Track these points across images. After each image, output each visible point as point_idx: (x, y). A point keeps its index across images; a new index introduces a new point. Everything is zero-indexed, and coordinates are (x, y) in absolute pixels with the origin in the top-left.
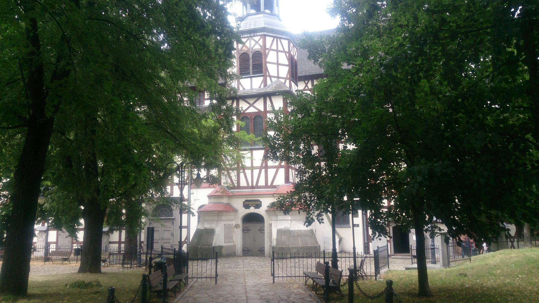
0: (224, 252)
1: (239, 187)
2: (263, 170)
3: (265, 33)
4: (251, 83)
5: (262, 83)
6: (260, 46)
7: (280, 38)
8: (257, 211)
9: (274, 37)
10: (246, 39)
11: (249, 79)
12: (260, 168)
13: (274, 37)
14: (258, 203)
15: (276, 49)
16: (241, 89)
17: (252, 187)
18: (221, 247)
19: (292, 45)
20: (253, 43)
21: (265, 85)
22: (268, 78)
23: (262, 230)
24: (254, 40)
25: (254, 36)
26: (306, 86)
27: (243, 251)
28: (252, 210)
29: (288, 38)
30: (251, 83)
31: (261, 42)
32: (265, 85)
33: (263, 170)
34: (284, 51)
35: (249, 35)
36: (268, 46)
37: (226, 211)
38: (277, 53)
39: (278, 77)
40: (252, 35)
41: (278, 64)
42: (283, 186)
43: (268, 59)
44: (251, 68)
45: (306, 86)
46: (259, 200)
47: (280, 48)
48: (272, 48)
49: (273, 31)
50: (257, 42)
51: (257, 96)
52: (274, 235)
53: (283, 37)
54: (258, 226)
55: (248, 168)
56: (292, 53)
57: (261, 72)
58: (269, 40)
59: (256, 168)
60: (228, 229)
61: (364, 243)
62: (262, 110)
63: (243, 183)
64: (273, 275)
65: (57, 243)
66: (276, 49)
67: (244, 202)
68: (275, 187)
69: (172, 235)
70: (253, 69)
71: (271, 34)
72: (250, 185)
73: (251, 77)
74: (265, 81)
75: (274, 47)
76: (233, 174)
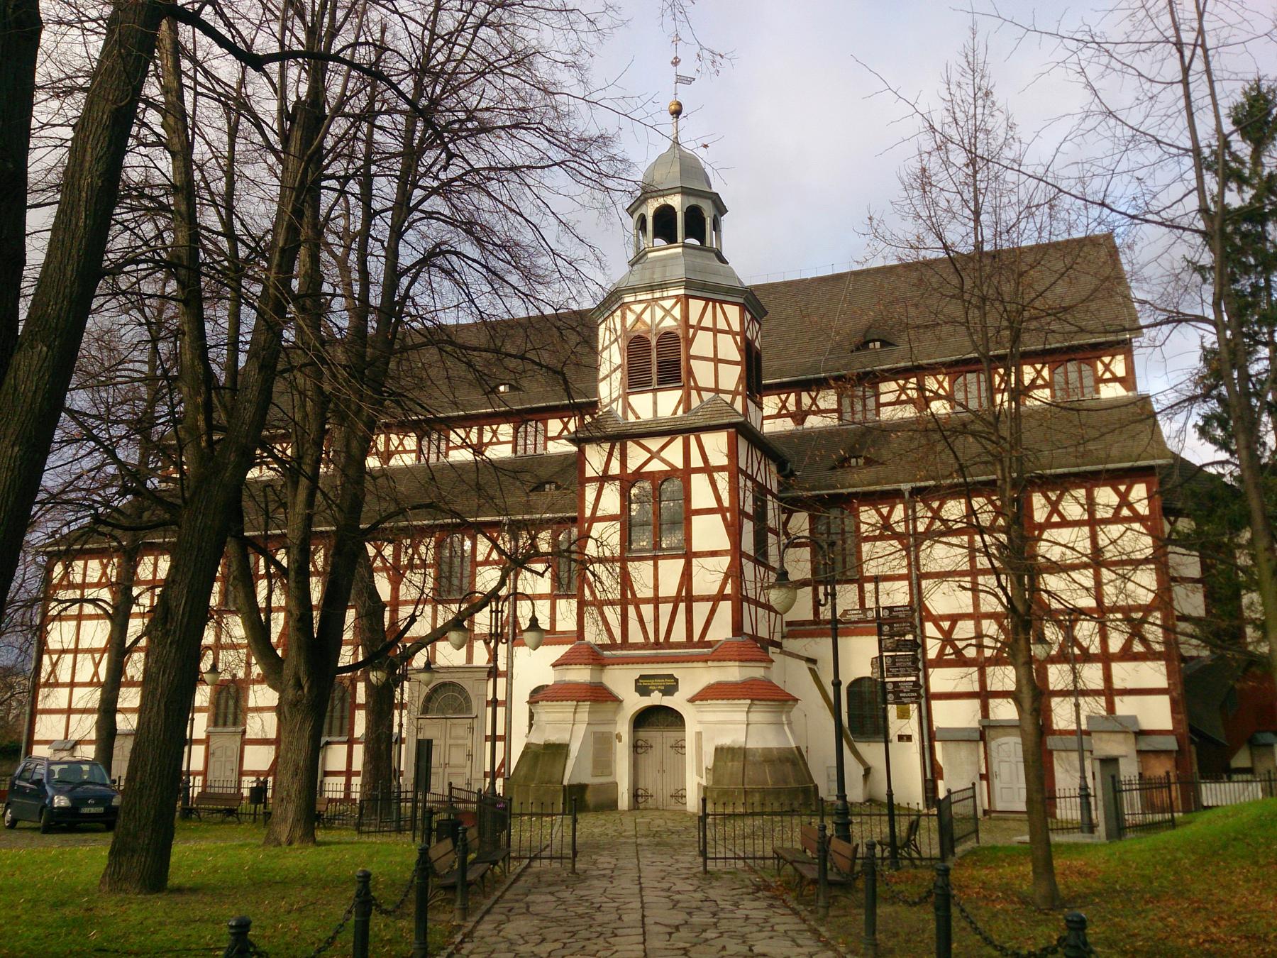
0: (590, 798)
1: (625, 644)
2: (682, 606)
4: (655, 403)
5: (679, 403)
6: (676, 319)
7: (721, 302)
8: (667, 701)
10: (643, 306)
11: (650, 395)
12: (676, 601)
13: (707, 300)
14: (670, 682)
16: (632, 418)
18: (582, 788)
19: (749, 316)
20: (659, 313)
22: (694, 393)
23: (679, 747)
25: (663, 298)
28: (656, 699)
30: (655, 403)
31: (677, 312)
32: (687, 409)
33: (682, 606)
36: (693, 321)
38: (715, 336)
39: (717, 390)
40: (657, 295)
41: (716, 361)
42: (727, 642)
43: (692, 352)
46: (671, 676)
47: (722, 325)
49: (704, 287)
50: (668, 312)
51: (669, 431)
52: (708, 760)
54: (671, 736)
55: (647, 601)
56: (748, 335)
57: (679, 380)
60: (602, 745)
61: (925, 781)
62: (680, 465)
63: (635, 636)
64: (703, 853)
65: (204, 773)
67: (637, 681)
68: (709, 644)
69: (470, 756)
70: (660, 372)
71: (698, 294)
72: (652, 639)
73: (654, 391)
74: (686, 400)
75: (707, 322)
76: (613, 615)
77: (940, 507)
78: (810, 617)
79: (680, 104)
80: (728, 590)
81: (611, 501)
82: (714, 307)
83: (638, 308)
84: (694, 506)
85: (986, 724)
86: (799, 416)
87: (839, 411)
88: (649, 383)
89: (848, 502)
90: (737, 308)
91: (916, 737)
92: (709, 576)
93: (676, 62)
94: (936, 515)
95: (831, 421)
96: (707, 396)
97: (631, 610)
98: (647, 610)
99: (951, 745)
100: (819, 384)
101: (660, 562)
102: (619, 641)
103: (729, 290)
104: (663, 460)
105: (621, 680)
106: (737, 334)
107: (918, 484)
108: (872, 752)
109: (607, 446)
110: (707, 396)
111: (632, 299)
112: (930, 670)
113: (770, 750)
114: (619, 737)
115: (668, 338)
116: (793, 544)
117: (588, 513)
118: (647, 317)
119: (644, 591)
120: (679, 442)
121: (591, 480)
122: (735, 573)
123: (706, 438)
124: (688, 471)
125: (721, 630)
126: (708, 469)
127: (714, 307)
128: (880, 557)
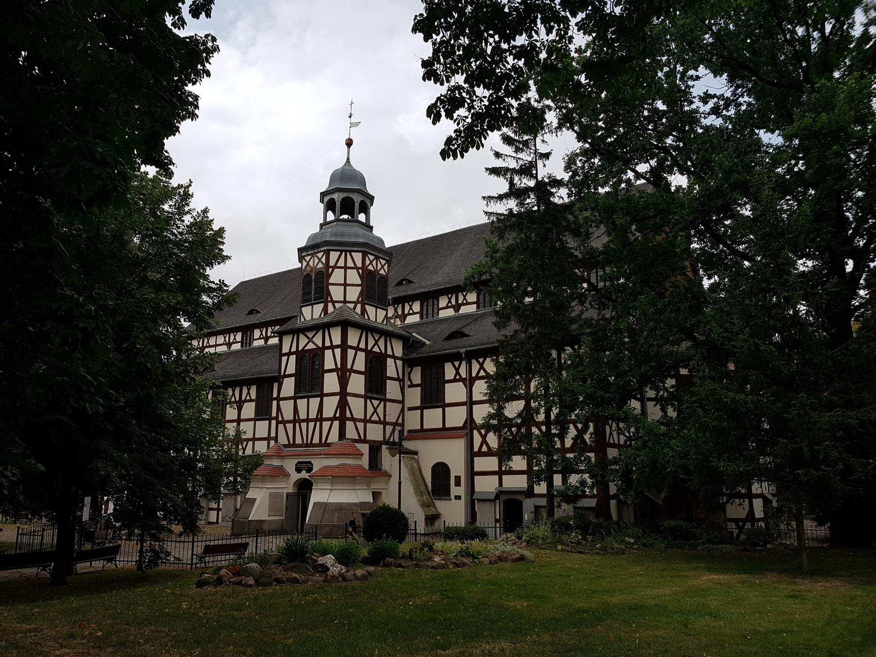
1: (294, 445)
3: (329, 248)
7: (350, 252)
12: (315, 420)
13: (341, 251)
14: (309, 465)
17: (307, 445)
18: (261, 522)
20: (317, 260)
21: (326, 313)
22: (330, 305)
25: (318, 252)
26: (450, 302)
28: (304, 475)
31: (323, 260)
32: (326, 313)
34: (355, 267)
36: (332, 263)
37: (270, 476)
41: (345, 285)
43: (330, 281)
45: (450, 302)
46: (310, 462)
49: (339, 244)
50: (320, 260)
57: (322, 297)
58: (334, 256)
59: (312, 420)
62: (321, 346)
63: (299, 441)
68: (329, 445)
71: (336, 248)
73: (312, 305)
74: (325, 309)
75: (341, 263)
76: (290, 427)
79: (351, 140)
80: (338, 415)
81: (291, 365)
82: (346, 255)
83: (307, 258)
87: (477, 303)
91: (463, 498)
92: (331, 406)
93: (350, 117)
94: (482, 367)
95: (472, 308)
99: (482, 503)
103: (354, 244)
104: (314, 343)
107: (469, 349)
108: (442, 506)
109: (290, 337)
110: (338, 305)
113: (341, 503)
115: (319, 273)
116: (412, 386)
118: (311, 263)
119: (303, 415)
120: (320, 334)
121: (285, 355)
123: (332, 330)
124: (324, 348)
125: (334, 437)
126: (332, 347)
127: (346, 255)
128: (454, 392)
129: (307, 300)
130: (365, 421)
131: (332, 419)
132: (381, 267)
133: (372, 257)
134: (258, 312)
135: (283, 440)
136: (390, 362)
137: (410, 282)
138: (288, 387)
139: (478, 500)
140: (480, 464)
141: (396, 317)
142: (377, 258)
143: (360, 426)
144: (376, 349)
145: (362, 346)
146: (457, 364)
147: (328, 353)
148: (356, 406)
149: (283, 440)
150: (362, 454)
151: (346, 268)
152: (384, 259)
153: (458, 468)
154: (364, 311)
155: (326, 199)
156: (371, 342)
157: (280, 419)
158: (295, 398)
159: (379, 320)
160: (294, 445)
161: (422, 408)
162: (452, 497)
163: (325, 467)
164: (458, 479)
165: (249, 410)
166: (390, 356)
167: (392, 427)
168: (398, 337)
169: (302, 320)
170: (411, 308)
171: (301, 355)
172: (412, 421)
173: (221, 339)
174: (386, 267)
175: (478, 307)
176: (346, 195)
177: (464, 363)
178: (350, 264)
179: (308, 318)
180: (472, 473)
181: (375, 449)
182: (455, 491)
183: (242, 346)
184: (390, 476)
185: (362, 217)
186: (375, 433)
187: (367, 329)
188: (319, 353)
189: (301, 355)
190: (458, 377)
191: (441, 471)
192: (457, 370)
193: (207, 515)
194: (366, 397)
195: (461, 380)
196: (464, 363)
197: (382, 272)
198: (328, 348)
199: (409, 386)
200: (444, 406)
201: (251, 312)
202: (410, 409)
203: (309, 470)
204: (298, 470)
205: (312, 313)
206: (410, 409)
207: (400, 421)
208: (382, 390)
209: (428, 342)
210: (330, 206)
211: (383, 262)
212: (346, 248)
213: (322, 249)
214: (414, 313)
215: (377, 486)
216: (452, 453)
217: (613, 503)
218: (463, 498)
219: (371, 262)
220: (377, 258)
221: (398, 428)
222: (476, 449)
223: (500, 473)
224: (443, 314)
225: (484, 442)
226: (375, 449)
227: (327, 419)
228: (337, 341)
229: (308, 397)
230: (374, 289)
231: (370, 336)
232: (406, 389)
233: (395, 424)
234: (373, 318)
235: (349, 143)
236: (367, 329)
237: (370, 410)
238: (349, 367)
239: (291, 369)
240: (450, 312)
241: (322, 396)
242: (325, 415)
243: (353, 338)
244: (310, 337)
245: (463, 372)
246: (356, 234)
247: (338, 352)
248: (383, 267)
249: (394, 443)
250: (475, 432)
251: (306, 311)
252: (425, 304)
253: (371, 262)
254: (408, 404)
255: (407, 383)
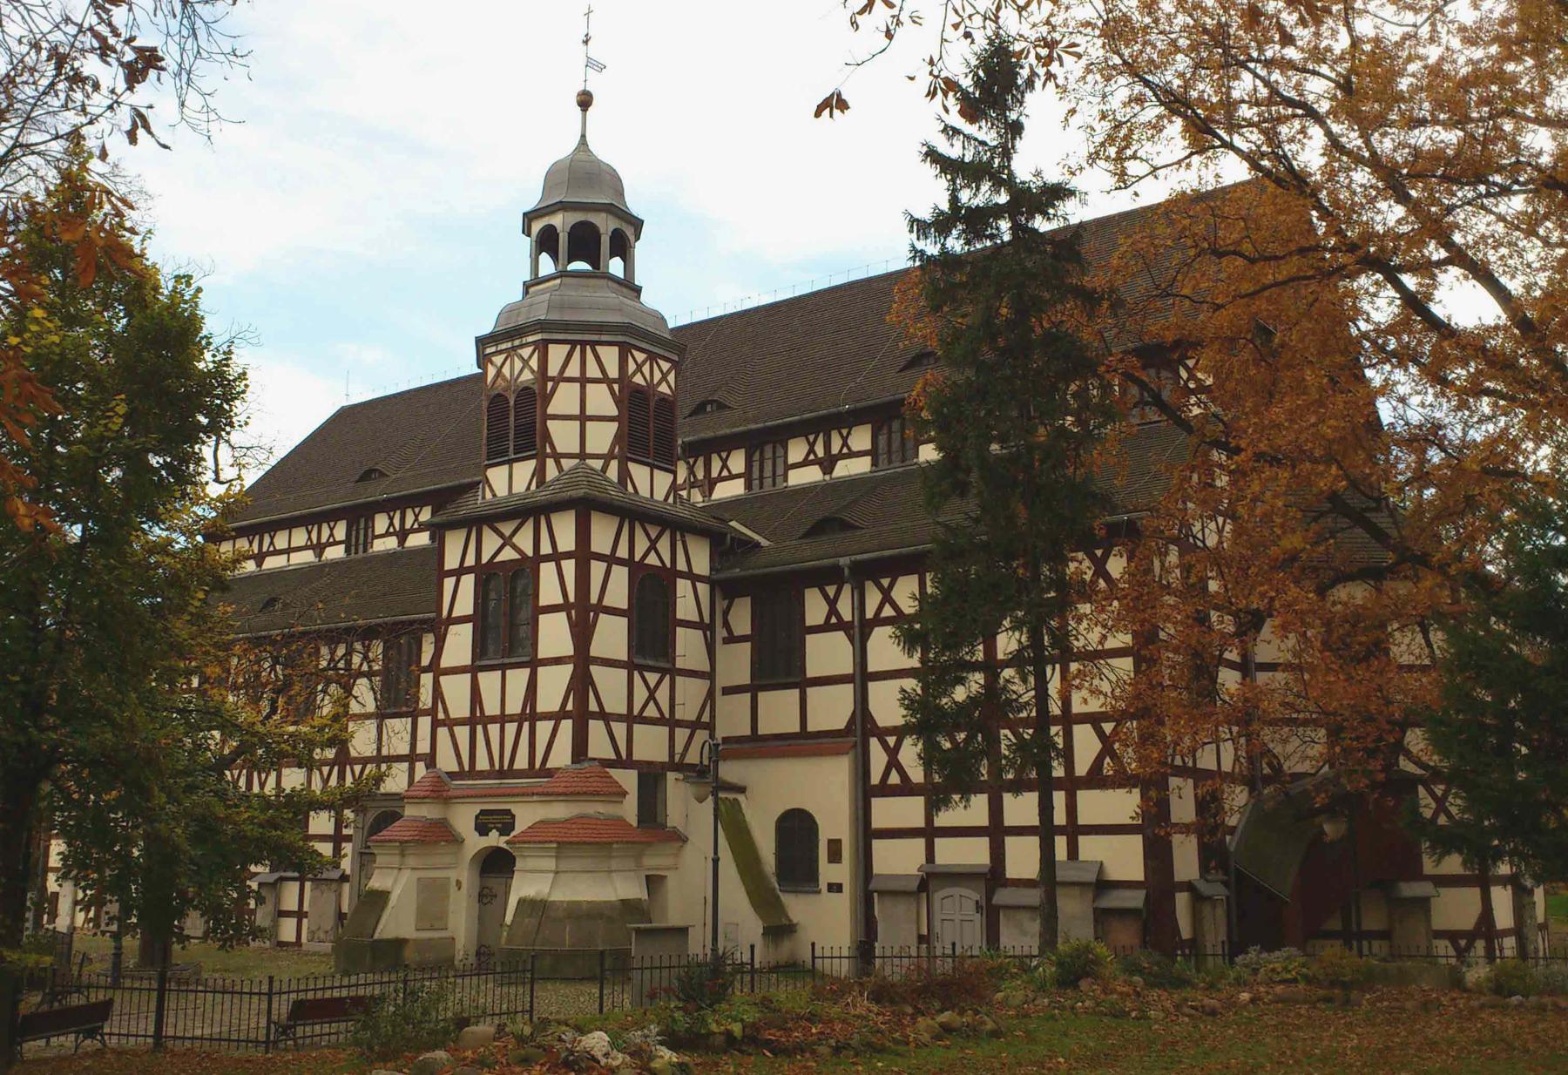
0: (410, 955)
1: (473, 773)
2: (526, 725)
7: (593, 344)
9: (573, 343)
12: (519, 719)
13: (573, 343)
14: (507, 819)
15: (577, 374)
17: (501, 774)
18: (400, 943)
20: (518, 364)
22: (550, 463)
24: (521, 358)
25: (522, 346)
26: (811, 451)
27: (478, 954)
28: (494, 839)
29: (620, 338)
31: (534, 363)
33: (526, 725)
34: (605, 379)
35: (509, 345)
36: (553, 371)
38: (583, 389)
39: (583, 455)
40: (517, 342)
41: (583, 418)
43: (550, 410)
44: (512, 436)
45: (811, 451)
46: (508, 812)
48: (567, 374)
49: (565, 327)
50: (525, 362)
53: (604, 338)
57: (532, 446)
58: (557, 354)
62: (530, 553)
63: (482, 764)
66: (577, 374)
68: (549, 773)
73: (510, 462)
74: (540, 472)
75: (573, 370)
77: (891, 585)
78: (748, 732)
80: (570, 707)
83: (498, 360)
84: (543, 602)
85: (930, 868)
86: (828, 464)
87: (873, 453)
88: (505, 452)
89: (797, 582)
90: (616, 349)
91: (846, 888)
93: (586, 42)
94: (887, 598)
95: (862, 466)
96: (567, 464)
97: (479, 728)
98: (494, 729)
100: (845, 421)
101: (508, 672)
102: (467, 768)
103: (601, 328)
104: (515, 547)
105: (463, 818)
106: (615, 381)
107: (859, 557)
109: (462, 534)
110: (567, 464)
111: (493, 349)
112: (874, 800)
113: (579, 903)
114: (459, 884)
116: (731, 639)
117: (445, 613)
118: (506, 371)
119: (491, 707)
121: (451, 573)
122: (581, 684)
124: (539, 558)
125: (561, 756)
126: (557, 557)
128: (827, 653)
129: (499, 454)
130: (631, 719)
131: (557, 717)
132: (661, 378)
133: (640, 357)
134: (382, 474)
135: (447, 762)
136: (683, 586)
137: (721, 406)
138: (459, 645)
139: (882, 893)
140: (886, 812)
141: (692, 486)
142: (652, 358)
143: (620, 729)
144: (652, 560)
145: (623, 552)
146: (831, 590)
147: (547, 571)
148: (611, 687)
149: (447, 762)
150: (624, 794)
151: (583, 381)
152: (667, 359)
153: (835, 822)
154: (624, 475)
155: (537, 227)
156: (642, 545)
157: (441, 716)
158: (473, 670)
159: (659, 495)
160: (473, 773)
161: (754, 689)
162: (823, 886)
163: (541, 822)
164: (835, 845)
165: (365, 695)
166: (683, 575)
167: (688, 731)
168: (701, 532)
169: (489, 495)
170: (725, 466)
171: (486, 574)
172: (733, 718)
173: (299, 537)
174: (671, 378)
175: (875, 463)
176: (578, 217)
177: (847, 589)
178: (593, 371)
179: (502, 491)
180: (866, 833)
181: (651, 778)
182: (828, 872)
183: (347, 550)
184: (685, 840)
185: (616, 266)
186: (651, 744)
187: (633, 514)
188: (527, 569)
189: (486, 574)
190: (834, 620)
191: (797, 829)
192: (832, 603)
193: (275, 926)
194: (630, 666)
195: (842, 626)
196: (847, 589)
197: (664, 388)
198: (547, 558)
199: (727, 641)
200: (803, 683)
201: (366, 476)
202: (728, 691)
203: (506, 828)
204: (482, 829)
205: (509, 480)
206: (728, 691)
207: (706, 718)
208: (665, 648)
209: (764, 542)
210: (546, 242)
211: (665, 366)
212: (584, 336)
213: (530, 339)
214: (732, 477)
215: (654, 861)
216: (824, 789)
217: (1182, 899)
218: (846, 888)
219: (639, 367)
220: (652, 358)
221: (701, 735)
222: (875, 779)
223: (930, 833)
224: (797, 478)
225: (893, 763)
226: (651, 778)
227: (547, 716)
228: (567, 542)
229: (503, 668)
230: (647, 427)
231: (639, 532)
232: (720, 649)
233: (694, 726)
234: (644, 491)
235: (585, 101)
236: (633, 514)
237: (641, 694)
238: (594, 599)
239: (465, 605)
240: (813, 475)
241: (534, 664)
242: (541, 707)
243: (602, 535)
244: (507, 533)
245: (845, 609)
246: (599, 304)
247: (569, 566)
248: (664, 377)
249: (692, 767)
250: (874, 742)
251: (498, 477)
252: (757, 456)
253: (639, 367)
254: (722, 681)
255: (721, 633)
